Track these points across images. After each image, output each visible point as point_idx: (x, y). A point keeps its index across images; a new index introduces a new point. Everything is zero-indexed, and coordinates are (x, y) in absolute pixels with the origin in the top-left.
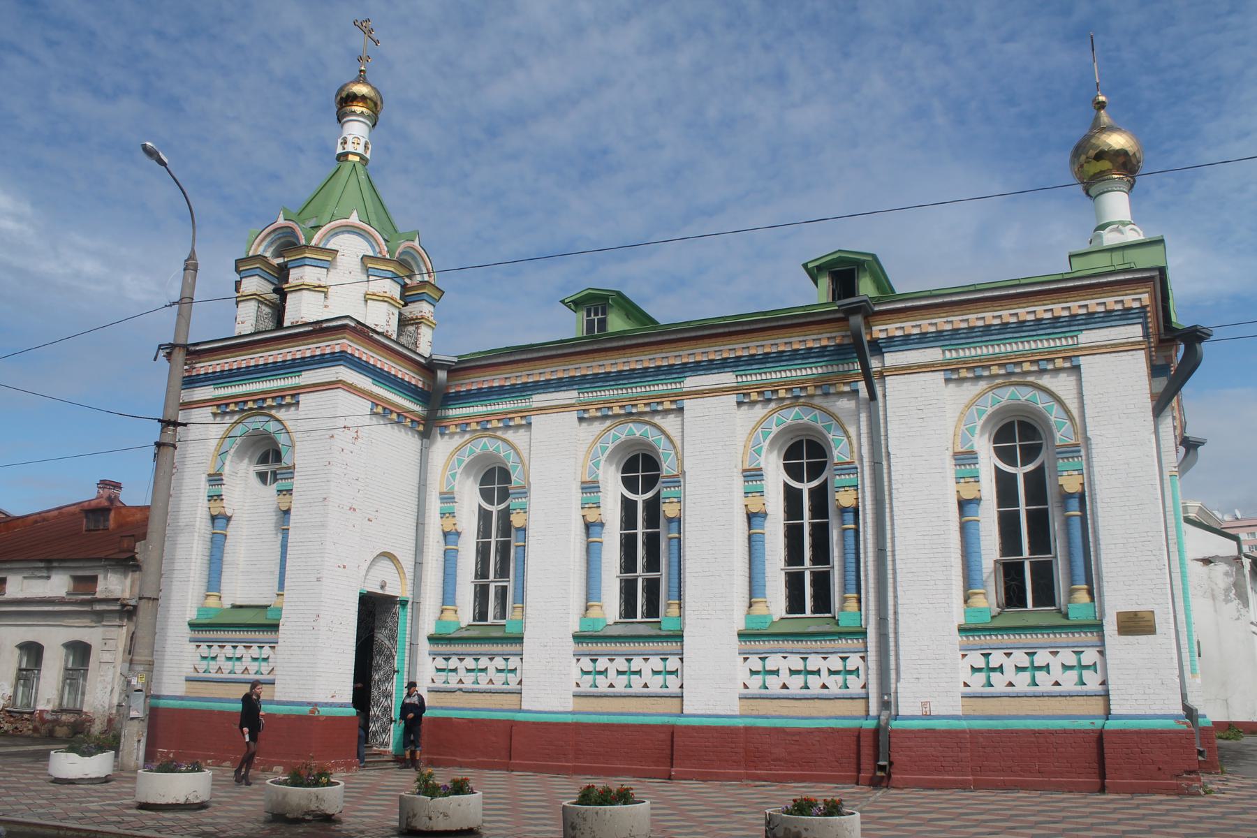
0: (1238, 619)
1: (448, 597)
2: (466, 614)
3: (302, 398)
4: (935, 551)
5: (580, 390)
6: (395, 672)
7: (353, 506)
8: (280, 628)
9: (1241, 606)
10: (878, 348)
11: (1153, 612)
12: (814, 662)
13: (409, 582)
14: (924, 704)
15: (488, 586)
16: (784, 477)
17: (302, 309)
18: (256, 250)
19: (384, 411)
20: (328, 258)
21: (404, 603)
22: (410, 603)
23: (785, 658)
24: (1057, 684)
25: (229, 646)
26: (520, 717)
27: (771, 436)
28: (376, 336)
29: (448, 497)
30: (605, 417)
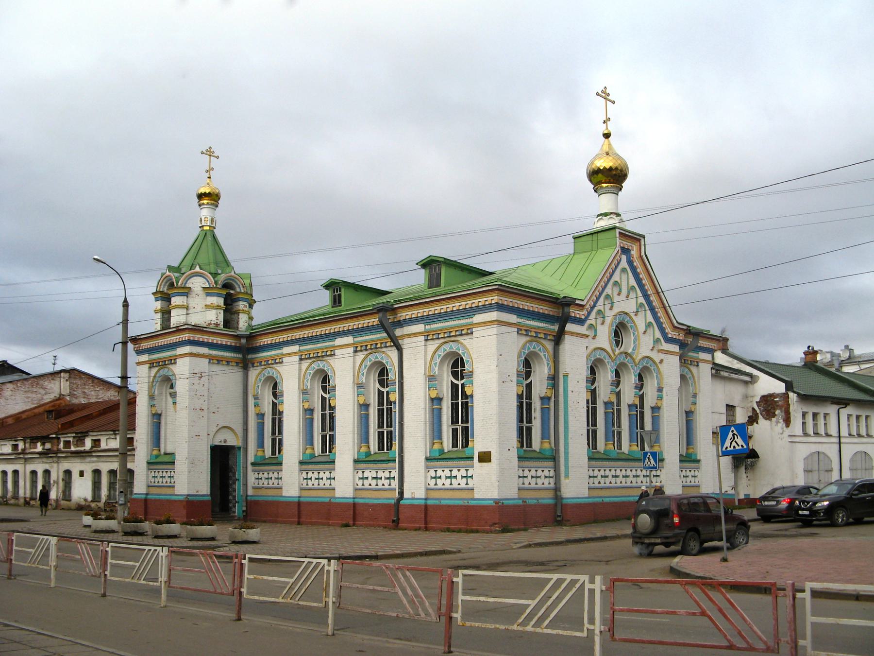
0: (782, 434)
1: (261, 444)
2: (268, 452)
3: (178, 360)
4: (418, 423)
5: (300, 345)
6: (237, 480)
7: (202, 408)
8: (176, 463)
9: (784, 425)
10: (400, 324)
11: (491, 452)
12: (380, 474)
13: (240, 439)
14: (413, 493)
15: (276, 439)
16: (378, 385)
17: (177, 318)
18: (160, 288)
19: (219, 361)
20: (186, 292)
21: (239, 448)
22: (242, 448)
23: (370, 471)
24: (459, 484)
25: (161, 471)
26: (281, 499)
27: (367, 367)
28: (204, 329)
29: (256, 398)
30: (310, 358)
